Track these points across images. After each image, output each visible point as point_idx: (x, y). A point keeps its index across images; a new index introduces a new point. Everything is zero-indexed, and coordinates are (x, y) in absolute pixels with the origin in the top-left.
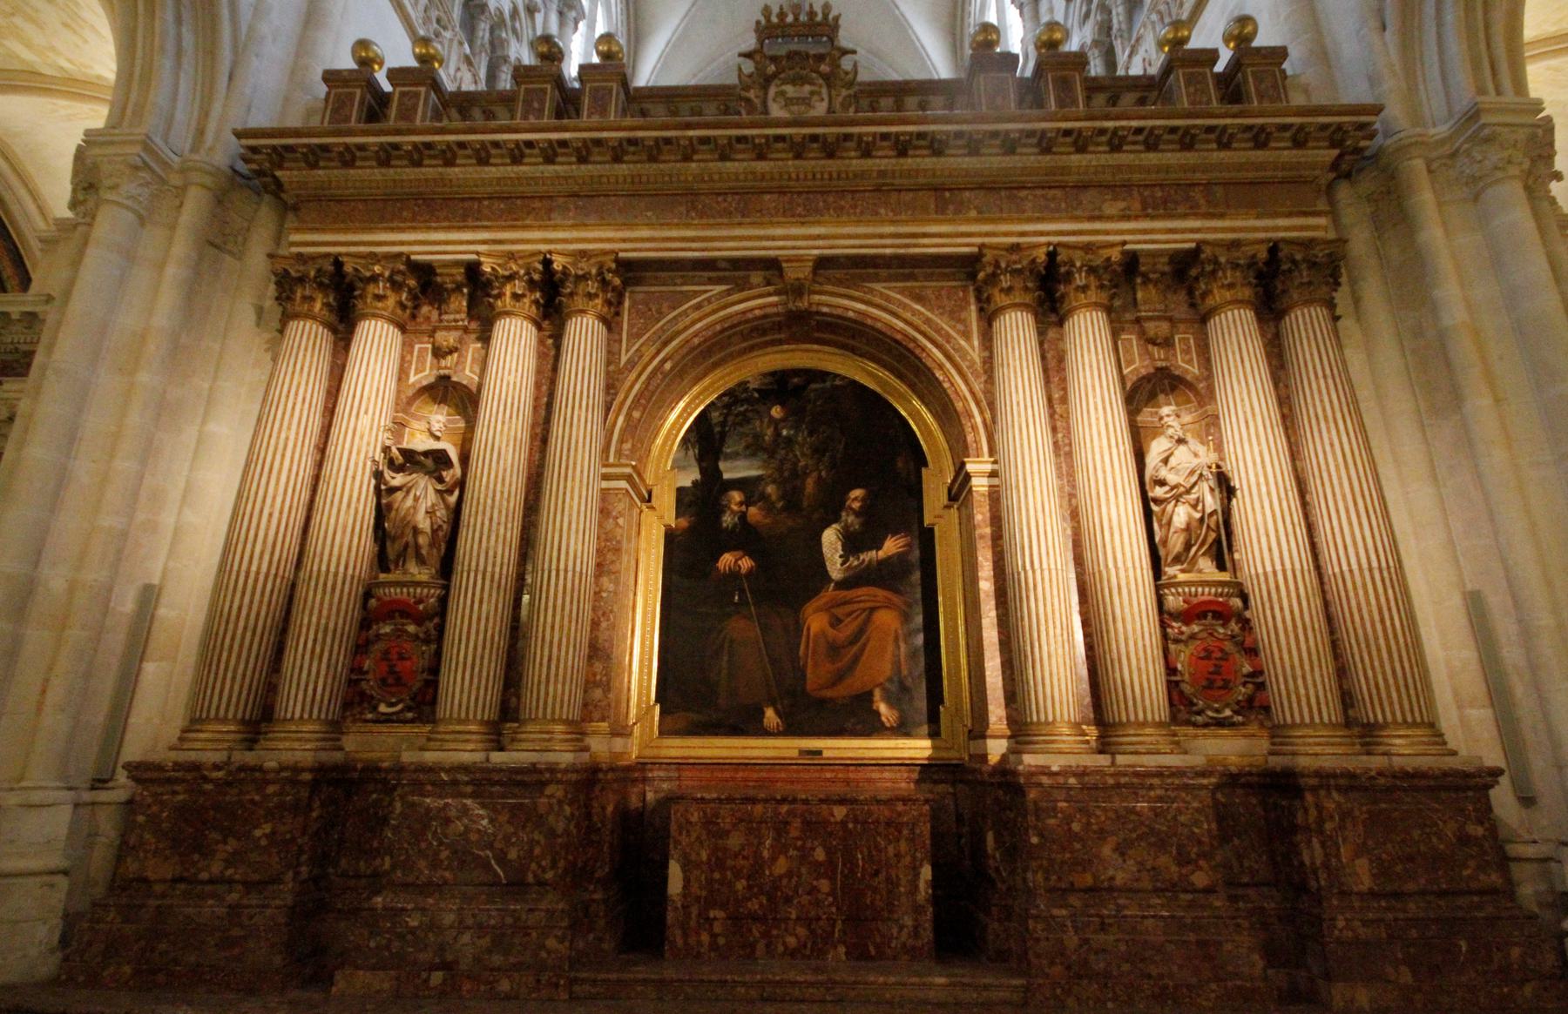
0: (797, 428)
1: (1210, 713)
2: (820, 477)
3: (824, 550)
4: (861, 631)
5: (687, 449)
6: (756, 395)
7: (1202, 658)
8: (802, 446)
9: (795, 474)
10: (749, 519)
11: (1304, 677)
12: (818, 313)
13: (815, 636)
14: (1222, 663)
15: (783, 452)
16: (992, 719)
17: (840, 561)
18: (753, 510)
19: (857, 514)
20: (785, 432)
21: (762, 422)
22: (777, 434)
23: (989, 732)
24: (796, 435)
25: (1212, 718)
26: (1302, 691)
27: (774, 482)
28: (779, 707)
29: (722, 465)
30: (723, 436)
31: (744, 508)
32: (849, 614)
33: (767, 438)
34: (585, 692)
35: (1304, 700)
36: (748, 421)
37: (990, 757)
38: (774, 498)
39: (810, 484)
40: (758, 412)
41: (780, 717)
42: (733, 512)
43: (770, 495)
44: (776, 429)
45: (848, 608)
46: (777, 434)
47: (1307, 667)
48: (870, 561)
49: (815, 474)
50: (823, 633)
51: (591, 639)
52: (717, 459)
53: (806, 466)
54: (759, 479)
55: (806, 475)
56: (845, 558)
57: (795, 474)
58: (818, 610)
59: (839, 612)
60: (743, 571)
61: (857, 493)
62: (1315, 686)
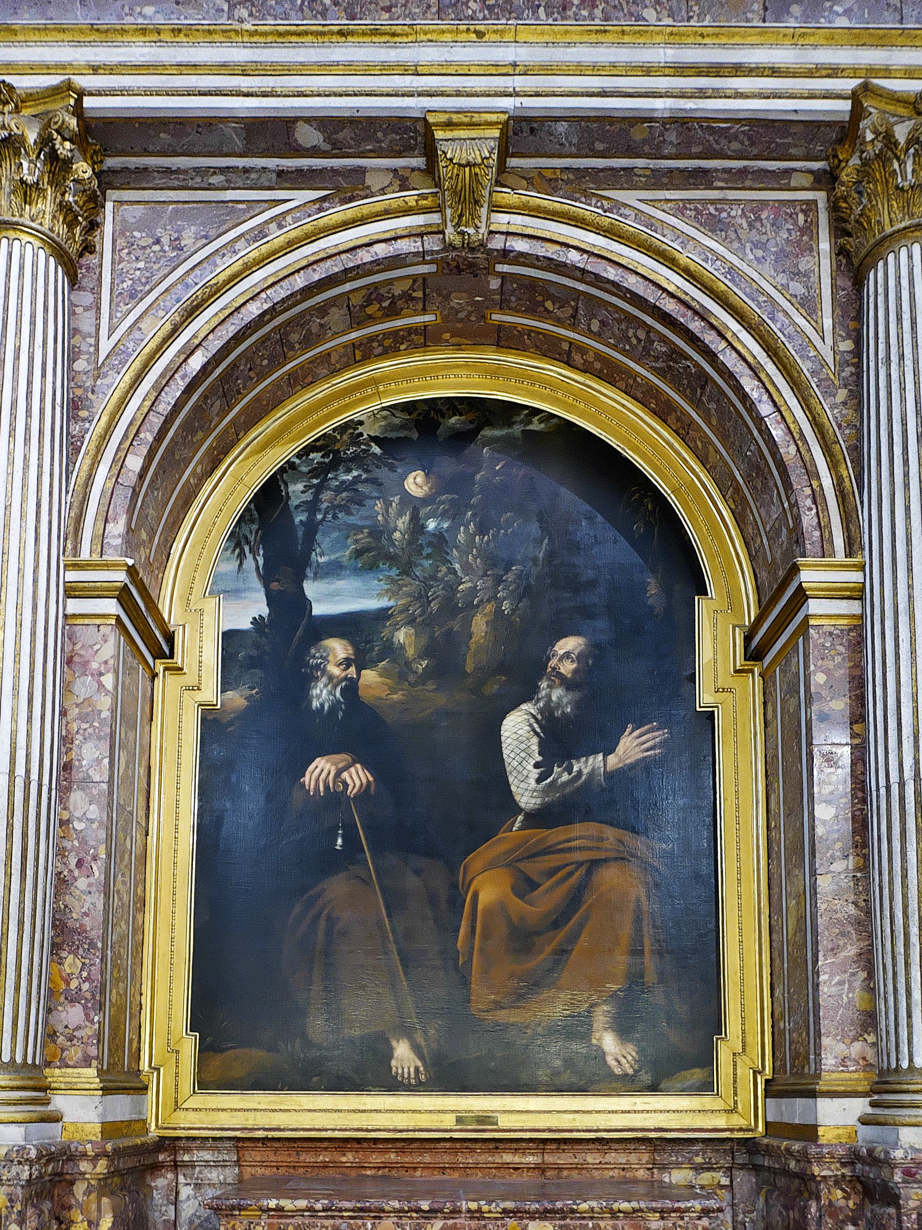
0: (455, 513)
2: (499, 611)
3: (506, 752)
4: (574, 901)
5: (241, 556)
6: (376, 450)
8: (465, 552)
9: (450, 607)
10: (360, 693)
12: (505, 255)
13: (488, 912)
15: (427, 563)
16: (829, 1061)
17: (535, 773)
18: (370, 676)
19: (568, 684)
20: (431, 525)
21: (388, 504)
22: (417, 527)
23: (822, 1086)
24: (454, 529)
27: (411, 622)
28: (421, 1041)
29: (310, 588)
30: (312, 528)
31: (352, 671)
32: (552, 873)
33: (397, 535)
34: (49, 1011)
36: (359, 501)
37: (821, 1131)
38: (411, 652)
39: (480, 625)
40: (375, 482)
41: (421, 1057)
42: (331, 678)
43: (402, 647)
44: (415, 518)
45: (553, 861)
46: (417, 527)
48: (592, 774)
49: (490, 608)
50: (502, 906)
51: (55, 911)
52: (301, 577)
53: (473, 591)
54: (382, 615)
55: (471, 608)
56: (545, 768)
57: (450, 607)
58: (491, 866)
59: (533, 868)
60: (352, 791)
61: (570, 644)
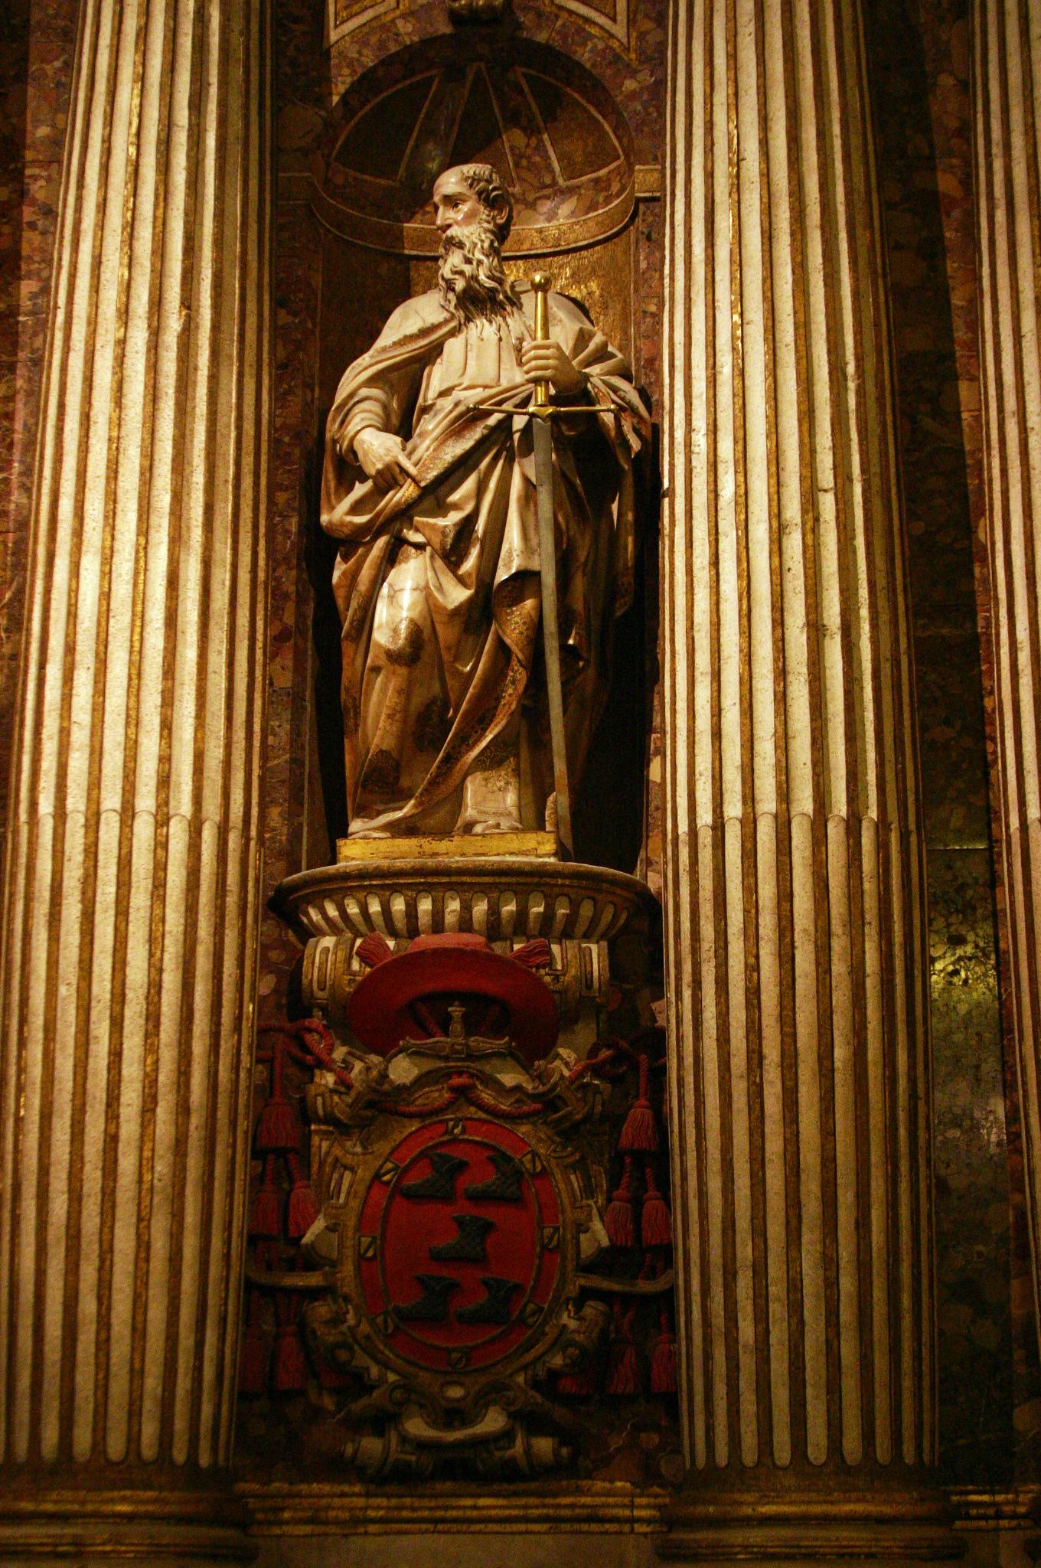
1: (417, 1427)
7: (414, 1196)
11: (760, 1269)
14: (490, 1213)
25: (423, 1446)
26: (747, 1330)
35: (747, 1363)
47: (776, 1230)
62: (795, 1308)
